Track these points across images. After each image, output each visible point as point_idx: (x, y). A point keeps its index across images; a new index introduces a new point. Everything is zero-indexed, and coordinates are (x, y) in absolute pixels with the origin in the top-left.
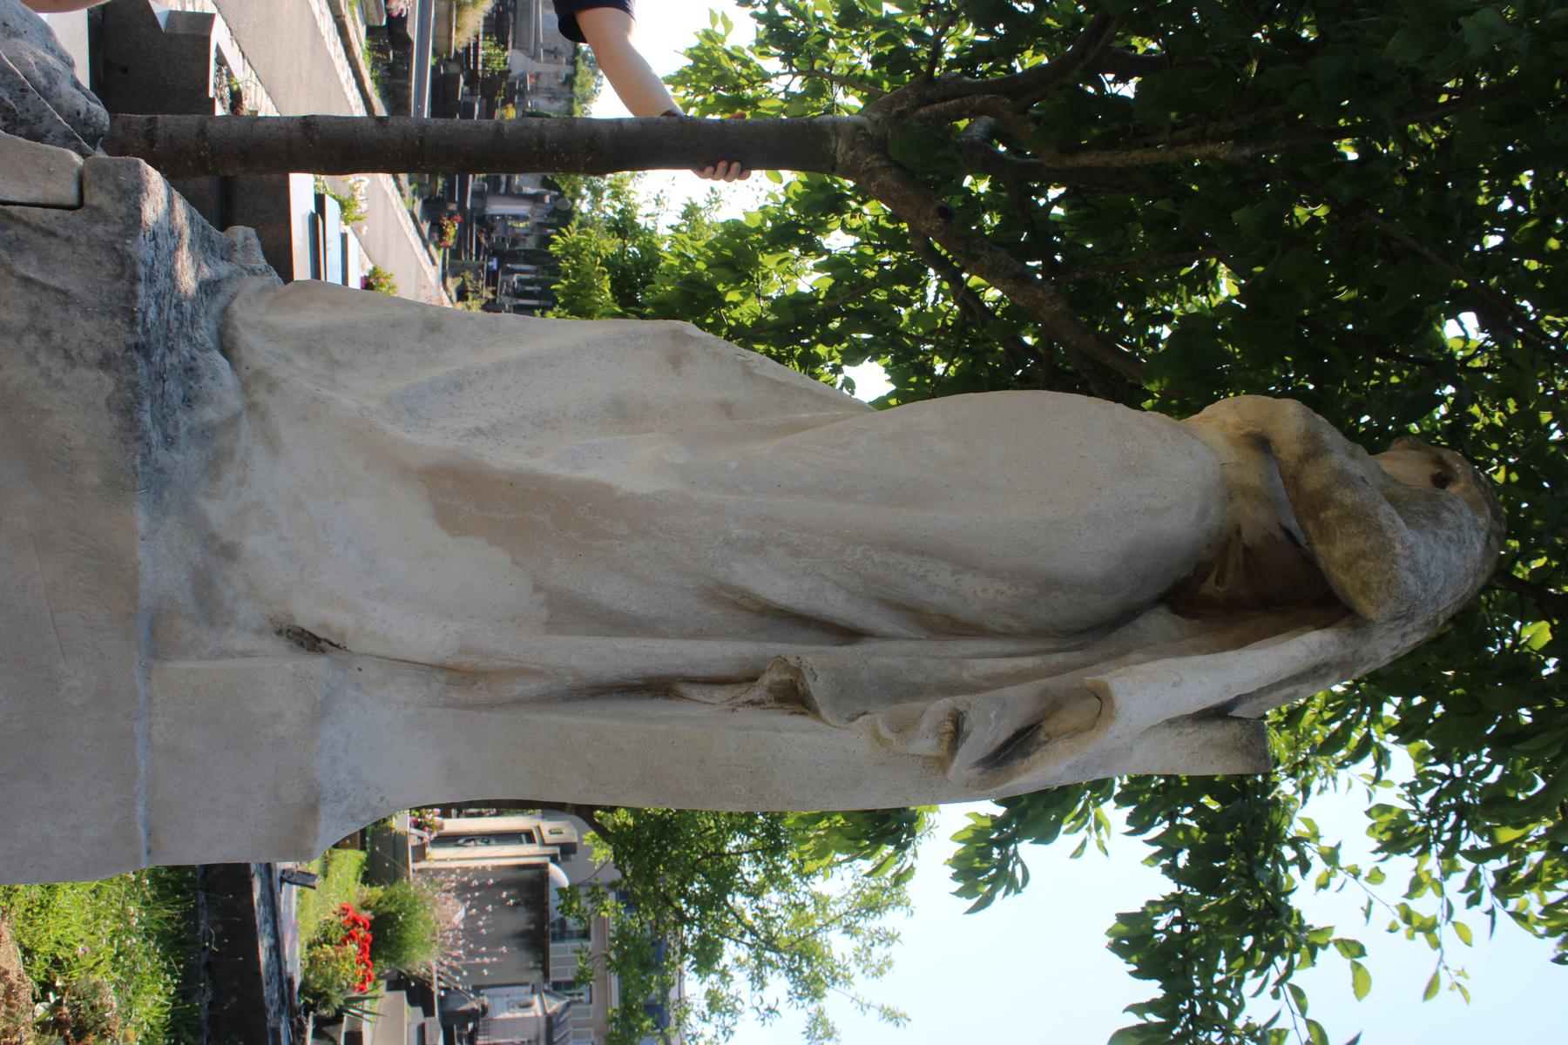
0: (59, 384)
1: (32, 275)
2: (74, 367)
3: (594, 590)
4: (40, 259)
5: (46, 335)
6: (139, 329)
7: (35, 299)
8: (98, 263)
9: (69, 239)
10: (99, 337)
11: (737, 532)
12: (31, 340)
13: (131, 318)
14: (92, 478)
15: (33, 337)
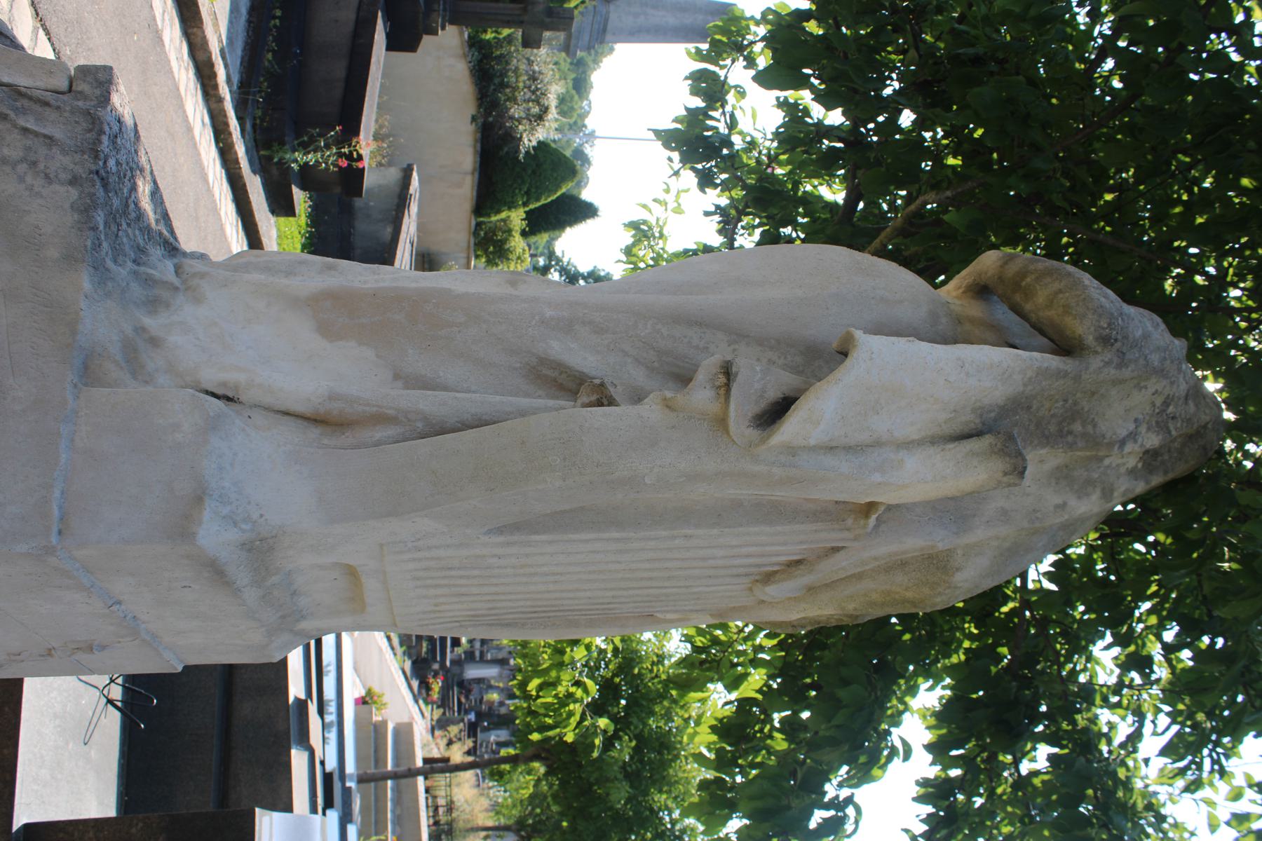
0: (39, 195)
1: (29, 126)
2: (50, 183)
3: (442, 374)
4: (36, 120)
5: (34, 164)
6: (101, 163)
7: (29, 143)
8: (77, 122)
9: (58, 108)
10: (72, 166)
11: (549, 313)
12: (22, 168)
13: (96, 154)
14: (53, 253)
15: (25, 165)
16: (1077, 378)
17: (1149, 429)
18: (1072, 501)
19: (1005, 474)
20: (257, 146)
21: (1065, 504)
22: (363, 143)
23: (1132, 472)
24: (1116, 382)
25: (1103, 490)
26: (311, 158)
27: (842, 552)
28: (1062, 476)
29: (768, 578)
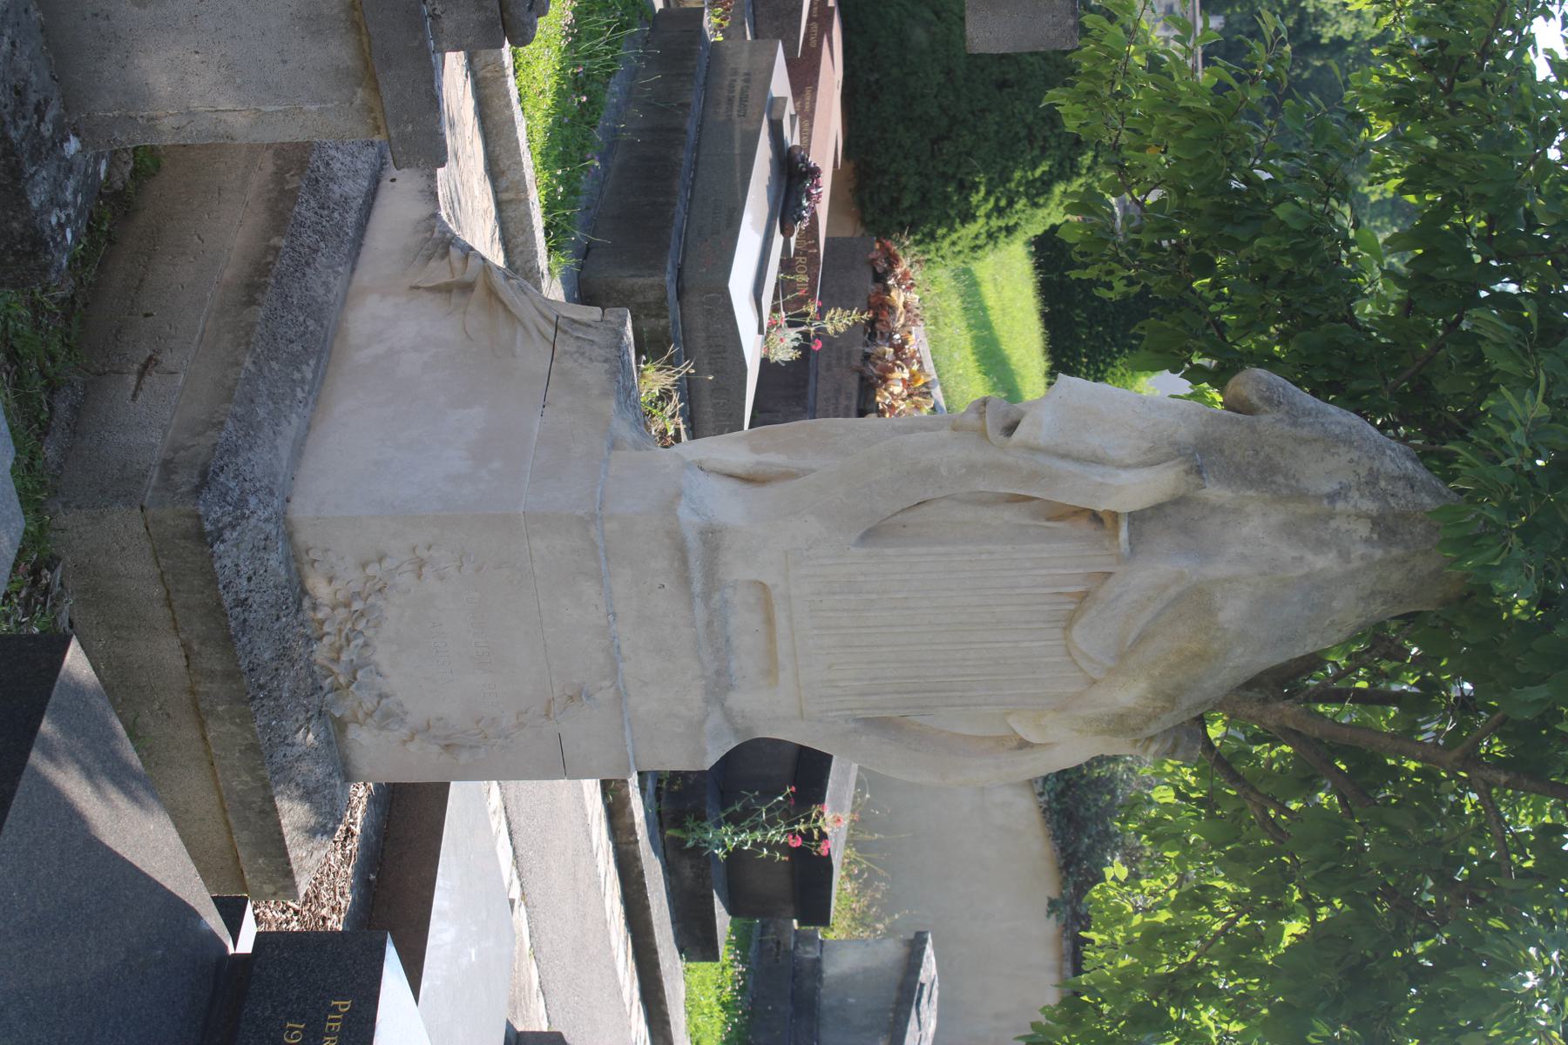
13: (619, 348)
16: (1253, 429)
17: (1362, 496)
18: (1309, 557)
19: (1187, 473)
20: (661, 824)
21: (1302, 558)
22: (828, 815)
23: (1367, 541)
24: (1303, 441)
25: (1340, 551)
26: (747, 838)
27: (1112, 579)
28: (1291, 530)
29: (1070, 621)
